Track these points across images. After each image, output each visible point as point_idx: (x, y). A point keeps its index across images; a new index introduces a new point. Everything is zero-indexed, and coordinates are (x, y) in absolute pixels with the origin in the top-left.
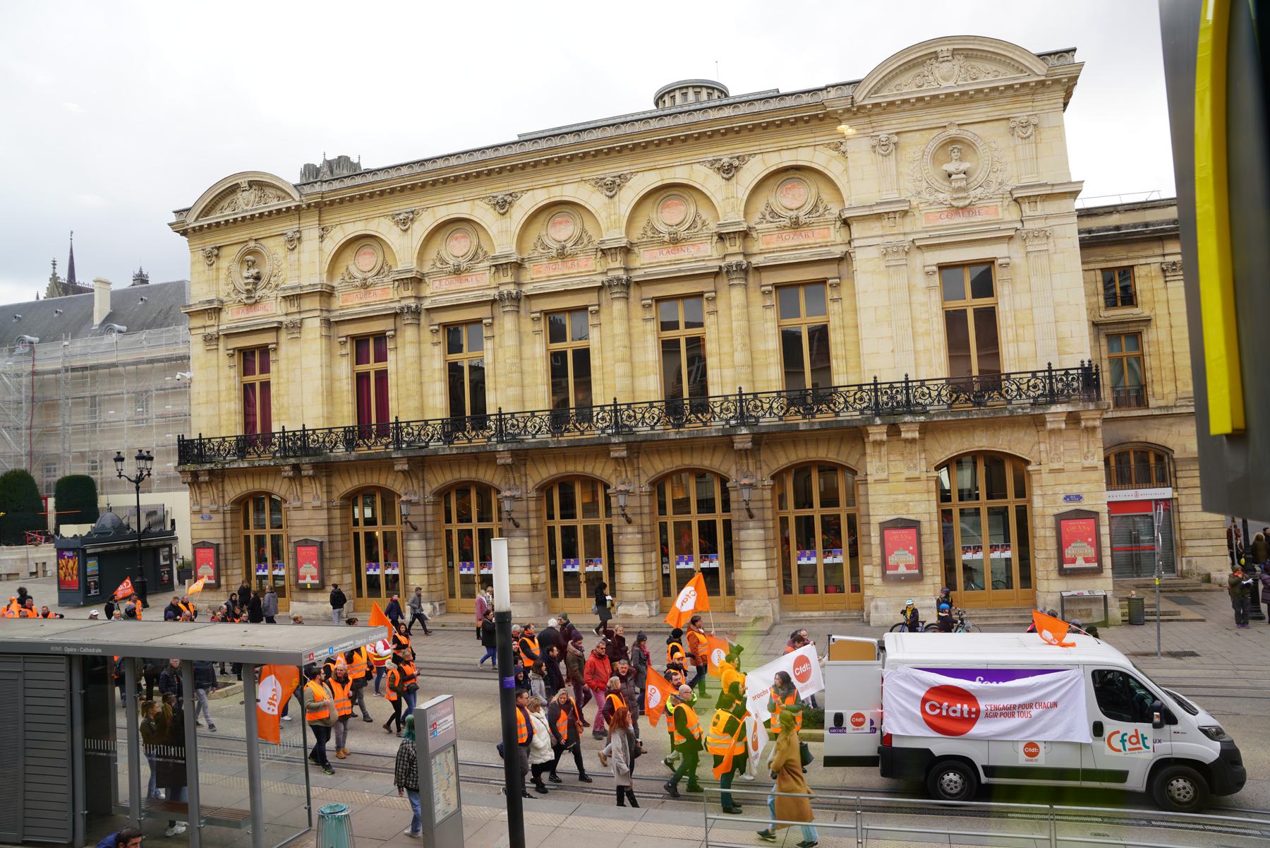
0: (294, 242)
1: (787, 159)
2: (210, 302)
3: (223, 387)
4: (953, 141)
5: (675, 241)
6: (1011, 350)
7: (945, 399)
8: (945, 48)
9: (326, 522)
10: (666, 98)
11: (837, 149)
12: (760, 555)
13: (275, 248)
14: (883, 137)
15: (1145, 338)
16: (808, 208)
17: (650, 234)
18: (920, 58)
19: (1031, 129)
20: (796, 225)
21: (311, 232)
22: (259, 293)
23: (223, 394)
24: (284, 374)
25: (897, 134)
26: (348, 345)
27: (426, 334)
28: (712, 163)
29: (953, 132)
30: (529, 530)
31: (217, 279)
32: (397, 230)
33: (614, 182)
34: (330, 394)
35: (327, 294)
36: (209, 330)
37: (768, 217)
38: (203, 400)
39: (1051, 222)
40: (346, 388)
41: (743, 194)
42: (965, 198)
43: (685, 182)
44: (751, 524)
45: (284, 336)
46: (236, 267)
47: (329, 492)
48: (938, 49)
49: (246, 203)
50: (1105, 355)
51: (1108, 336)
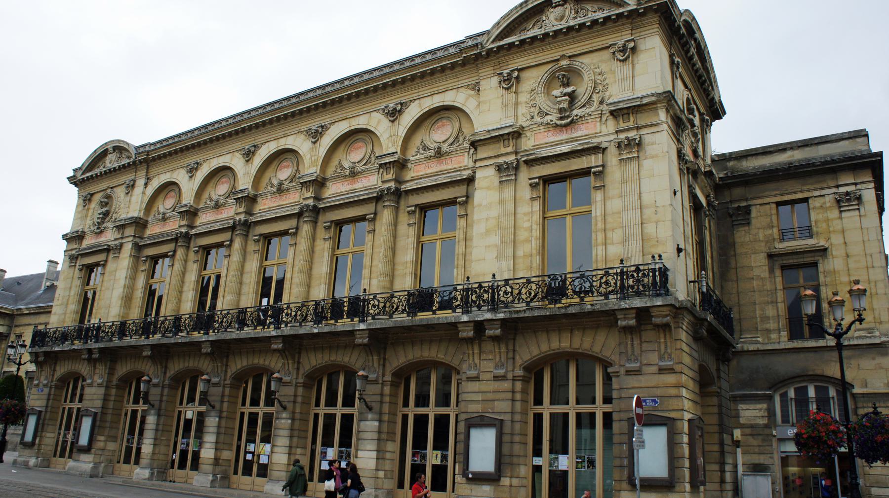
0: (131, 186)
1: (437, 101)
2: (77, 231)
3: (72, 293)
5: (354, 174)
6: (600, 252)
7: (524, 297)
9: (102, 397)
11: (473, 89)
12: (372, 446)
13: (120, 192)
15: (821, 267)
16: (451, 140)
17: (339, 171)
20: (439, 154)
21: (141, 182)
22: (105, 225)
23: (71, 298)
24: (105, 284)
26: (147, 264)
27: (192, 255)
28: (384, 110)
30: (221, 411)
31: (86, 216)
32: (187, 176)
33: (317, 131)
34: (127, 299)
35: (140, 224)
36: (74, 252)
37: (421, 151)
38: (60, 302)
39: (642, 132)
40: (139, 294)
41: (402, 131)
42: (568, 117)
43: (364, 127)
44: (370, 416)
45: (111, 256)
46: (98, 207)
47: (111, 373)
49: (111, 162)
50: (780, 286)
51: (783, 268)
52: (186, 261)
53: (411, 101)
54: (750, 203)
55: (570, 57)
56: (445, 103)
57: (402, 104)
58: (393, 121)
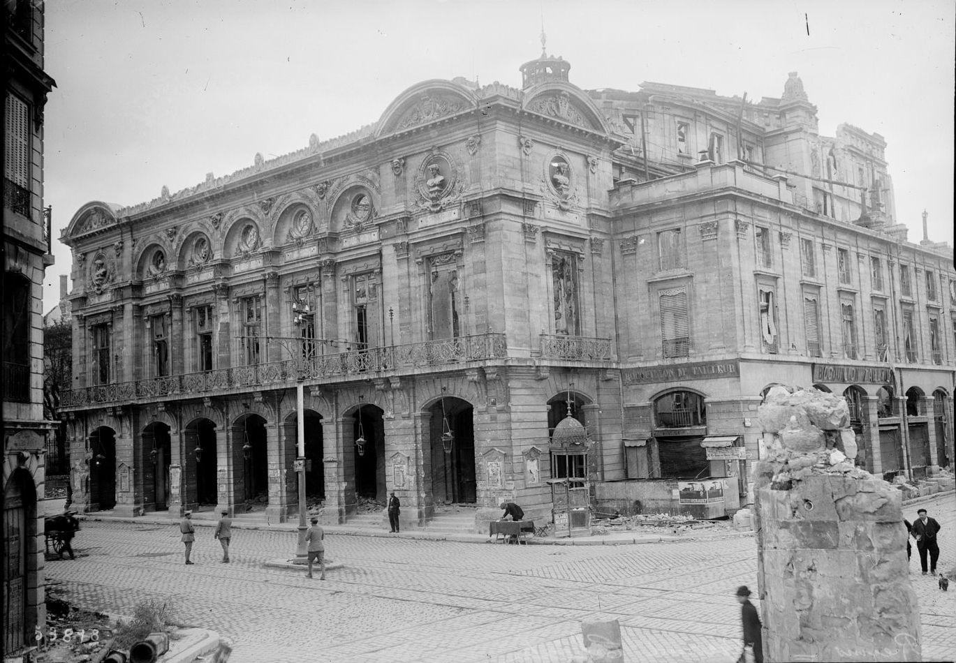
0: (120, 249)
18: (411, 103)
21: (128, 243)
27: (187, 317)
52: (182, 320)
54: (637, 233)
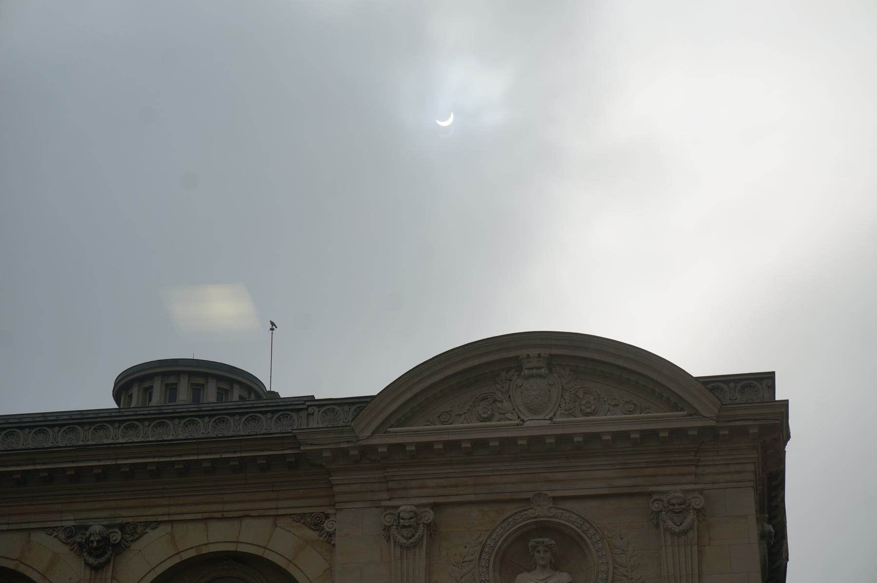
4: (543, 528)
8: (533, 352)
10: (135, 391)
11: (317, 525)
14: (406, 507)
19: (691, 516)
25: (435, 506)
28: (70, 533)
29: (542, 511)
48: (522, 353)
53: (147, 524)
55: (555, 499)
56: (242, 548)
57: (122, 527)
58: (96, 569)
